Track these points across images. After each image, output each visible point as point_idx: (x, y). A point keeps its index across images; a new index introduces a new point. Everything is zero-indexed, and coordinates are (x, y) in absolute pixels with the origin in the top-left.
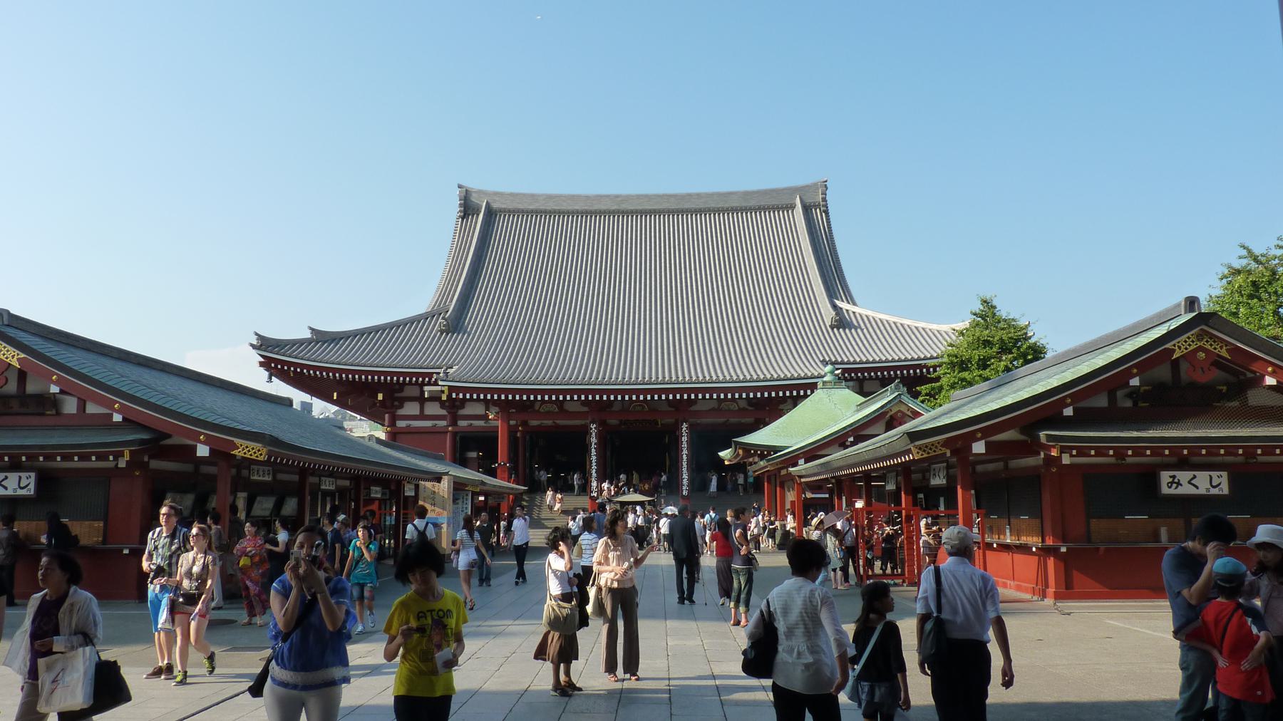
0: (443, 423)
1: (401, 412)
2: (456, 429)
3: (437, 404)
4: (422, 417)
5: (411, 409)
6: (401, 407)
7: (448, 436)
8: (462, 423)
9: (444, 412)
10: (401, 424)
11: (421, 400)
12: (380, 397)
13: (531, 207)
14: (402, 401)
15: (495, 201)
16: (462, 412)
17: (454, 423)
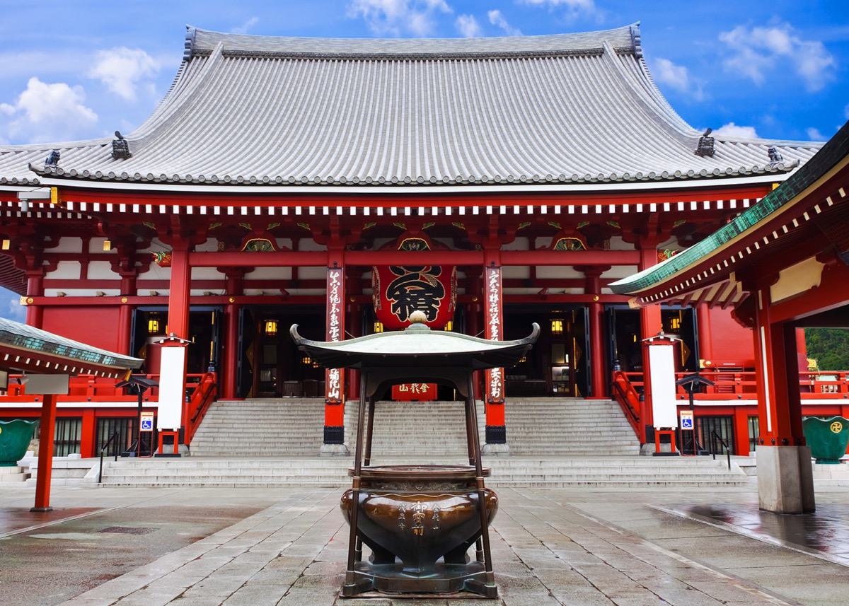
0: (117, 292)
1: (51, 276)
2: (134, 301)
3: (107, 265)
4: (84, 282)
5: (68, 270)
6: (54, 268)
7: (125, 310)
8: (142, 292)
9: (117, 276)
10: (50, 293)
11: (85, 258)
12: (6, 245)
13: (275, 51)
14: (56, 259)
15: (231, 43)
16: (144, 276)
17: (133, 293)
